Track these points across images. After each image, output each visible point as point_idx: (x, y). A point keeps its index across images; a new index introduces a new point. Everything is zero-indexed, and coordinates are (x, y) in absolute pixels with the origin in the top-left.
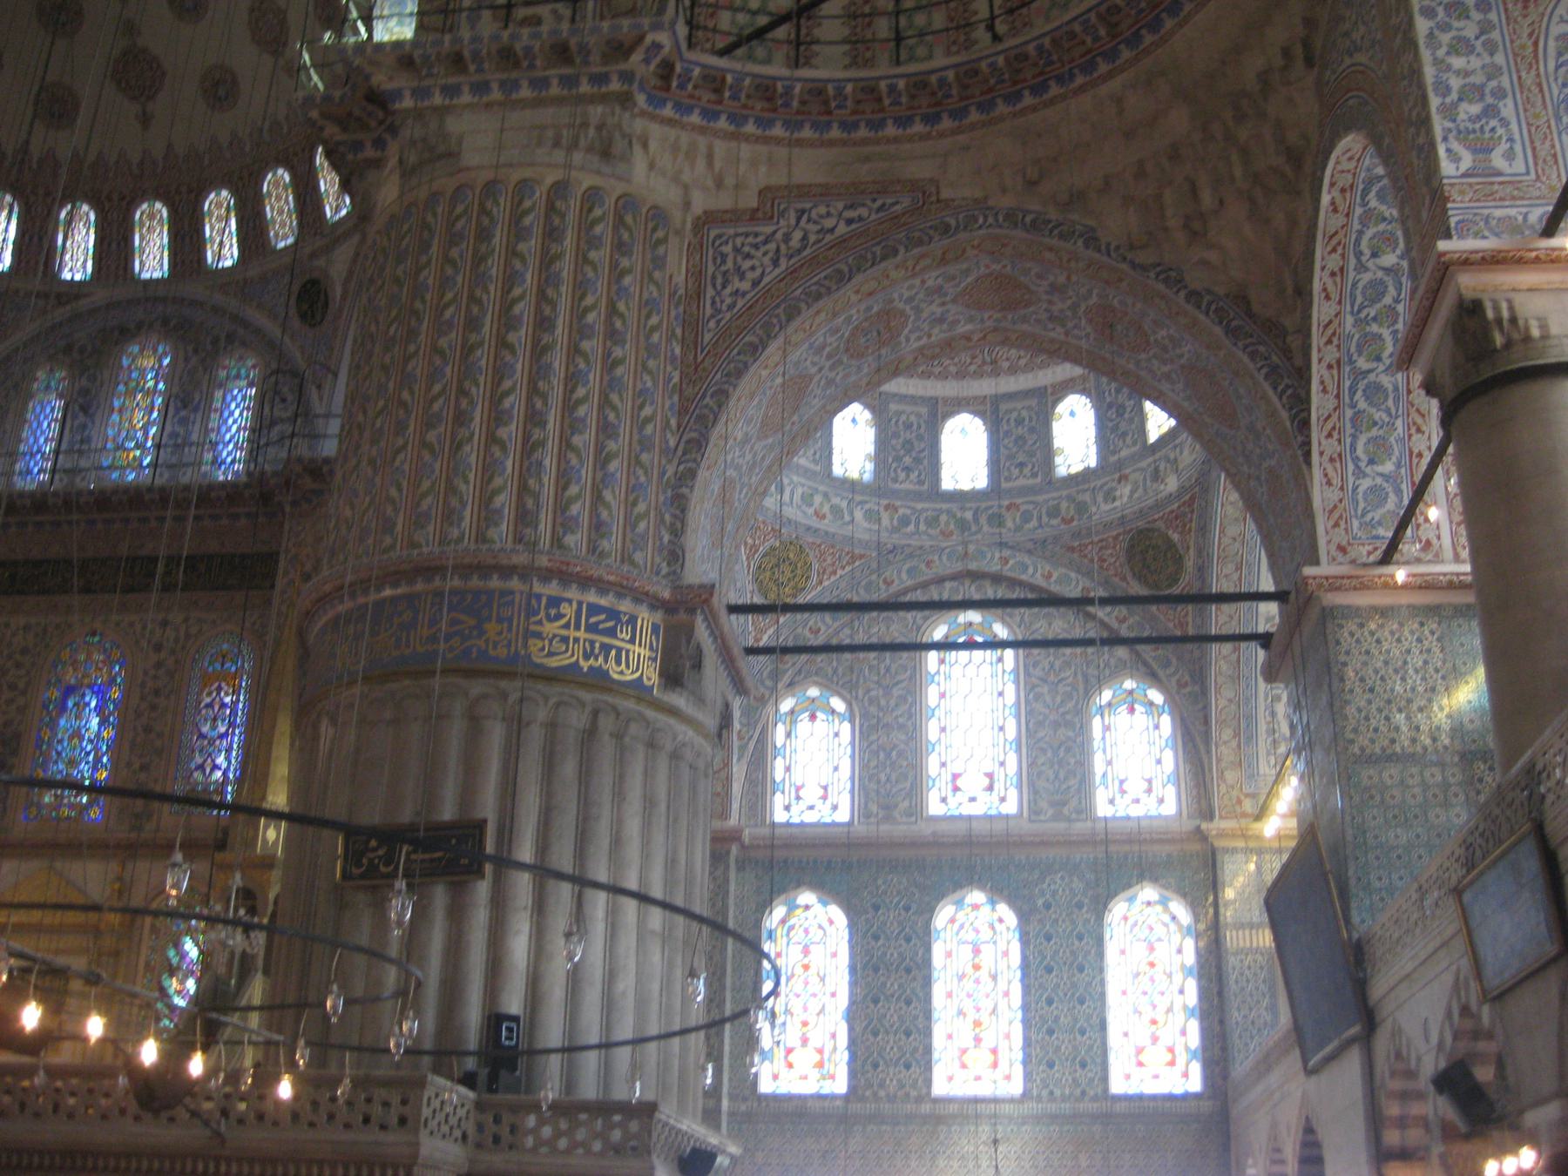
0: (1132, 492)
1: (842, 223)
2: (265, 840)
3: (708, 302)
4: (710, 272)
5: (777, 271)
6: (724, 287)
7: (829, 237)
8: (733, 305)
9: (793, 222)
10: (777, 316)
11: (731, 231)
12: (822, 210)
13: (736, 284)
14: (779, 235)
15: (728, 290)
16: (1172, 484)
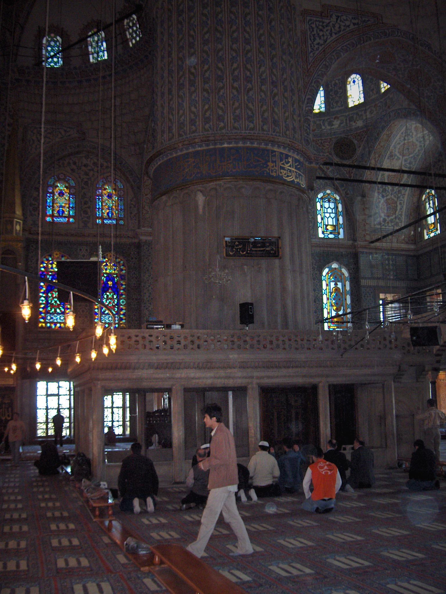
0: (341, 123)
1: (352, 24)
2: (16, 230)
3: (309, 46)
4: (308, 35)
5: (332, 38)
6: (314, 41)
7: (348, 29)
8: (317, 49)
9: (335, 20)
10: (333, 56)
11: (315, 19)
12: (344, 17)
13: (318, 41)
14: (331, 24)
15: (315, 43)
16: (360, 123)
